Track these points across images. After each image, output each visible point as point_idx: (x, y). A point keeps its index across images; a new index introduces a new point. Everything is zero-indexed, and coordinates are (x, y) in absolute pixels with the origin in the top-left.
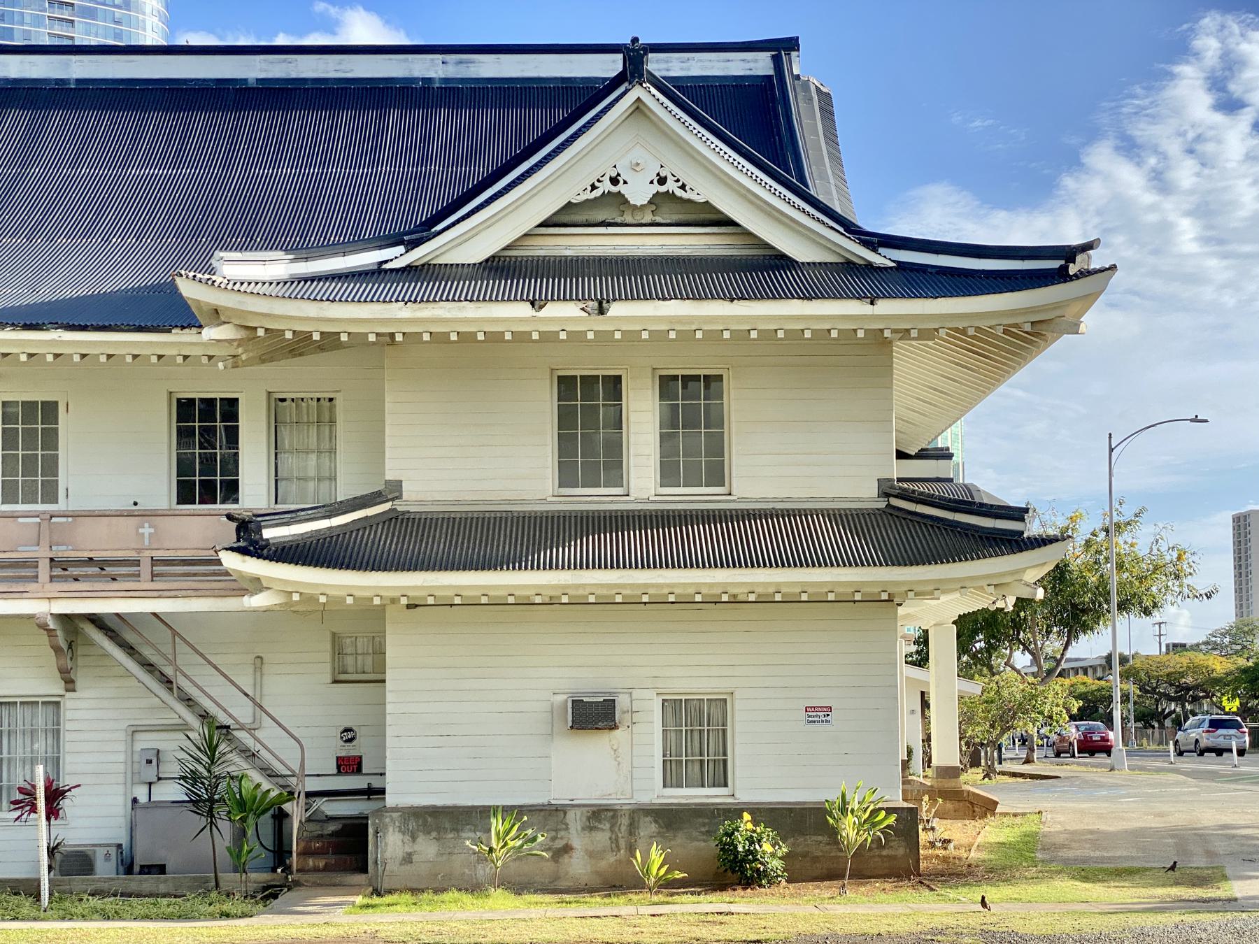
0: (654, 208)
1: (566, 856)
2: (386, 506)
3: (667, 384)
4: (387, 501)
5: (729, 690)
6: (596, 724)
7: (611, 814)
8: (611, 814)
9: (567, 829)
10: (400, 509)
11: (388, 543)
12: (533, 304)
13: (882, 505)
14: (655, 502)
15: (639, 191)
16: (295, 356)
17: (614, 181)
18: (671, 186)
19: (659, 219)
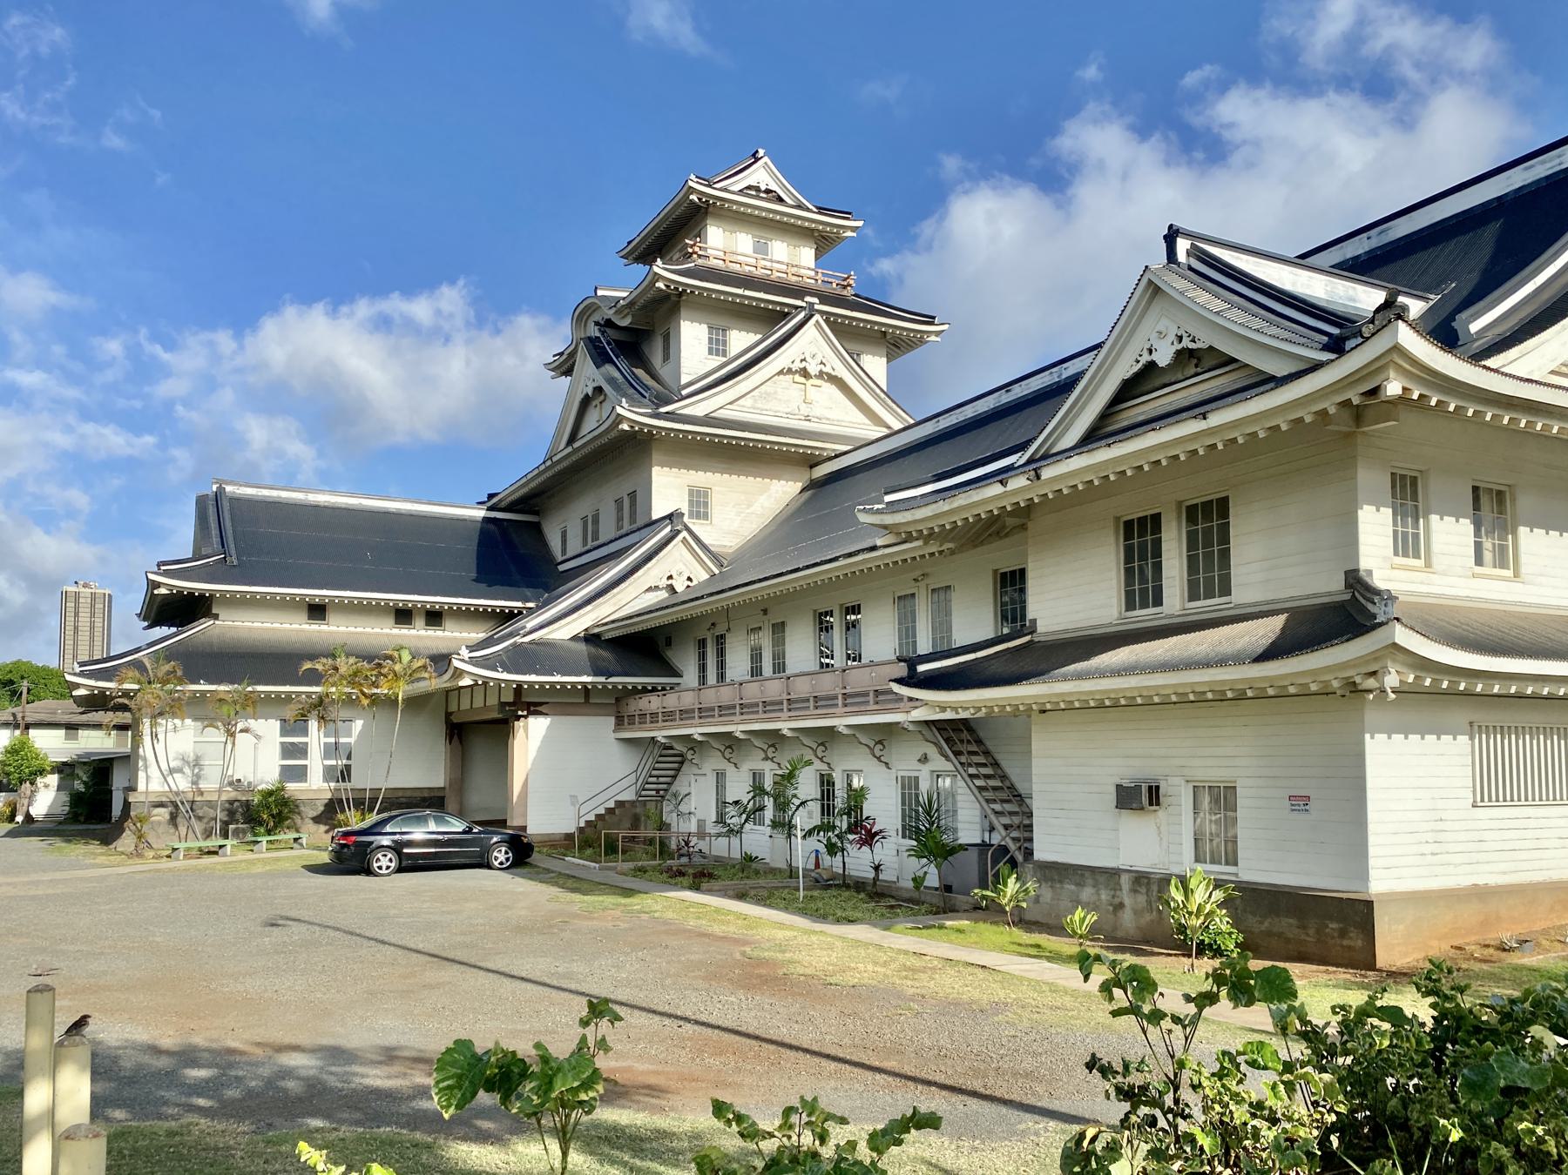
0: (1195, 361)
1: (1121, 912)
2: (1027, 638)
3: (1192, 513)
4: (1026, 635)
5: (1233, 779)
6: (1131, 803)
7: (1146, 881)
8: (1146, 881)
9: (1121, 890)
10: (1036, 640)
11: (997, 668)
12: (1001, 482)
13: (1347, 597)
14: (1179, 616)
15: (1163, 358)
16: (1001, 538)
17: (1150, 352)
18: (1186, 343)
19: (1199, 370)
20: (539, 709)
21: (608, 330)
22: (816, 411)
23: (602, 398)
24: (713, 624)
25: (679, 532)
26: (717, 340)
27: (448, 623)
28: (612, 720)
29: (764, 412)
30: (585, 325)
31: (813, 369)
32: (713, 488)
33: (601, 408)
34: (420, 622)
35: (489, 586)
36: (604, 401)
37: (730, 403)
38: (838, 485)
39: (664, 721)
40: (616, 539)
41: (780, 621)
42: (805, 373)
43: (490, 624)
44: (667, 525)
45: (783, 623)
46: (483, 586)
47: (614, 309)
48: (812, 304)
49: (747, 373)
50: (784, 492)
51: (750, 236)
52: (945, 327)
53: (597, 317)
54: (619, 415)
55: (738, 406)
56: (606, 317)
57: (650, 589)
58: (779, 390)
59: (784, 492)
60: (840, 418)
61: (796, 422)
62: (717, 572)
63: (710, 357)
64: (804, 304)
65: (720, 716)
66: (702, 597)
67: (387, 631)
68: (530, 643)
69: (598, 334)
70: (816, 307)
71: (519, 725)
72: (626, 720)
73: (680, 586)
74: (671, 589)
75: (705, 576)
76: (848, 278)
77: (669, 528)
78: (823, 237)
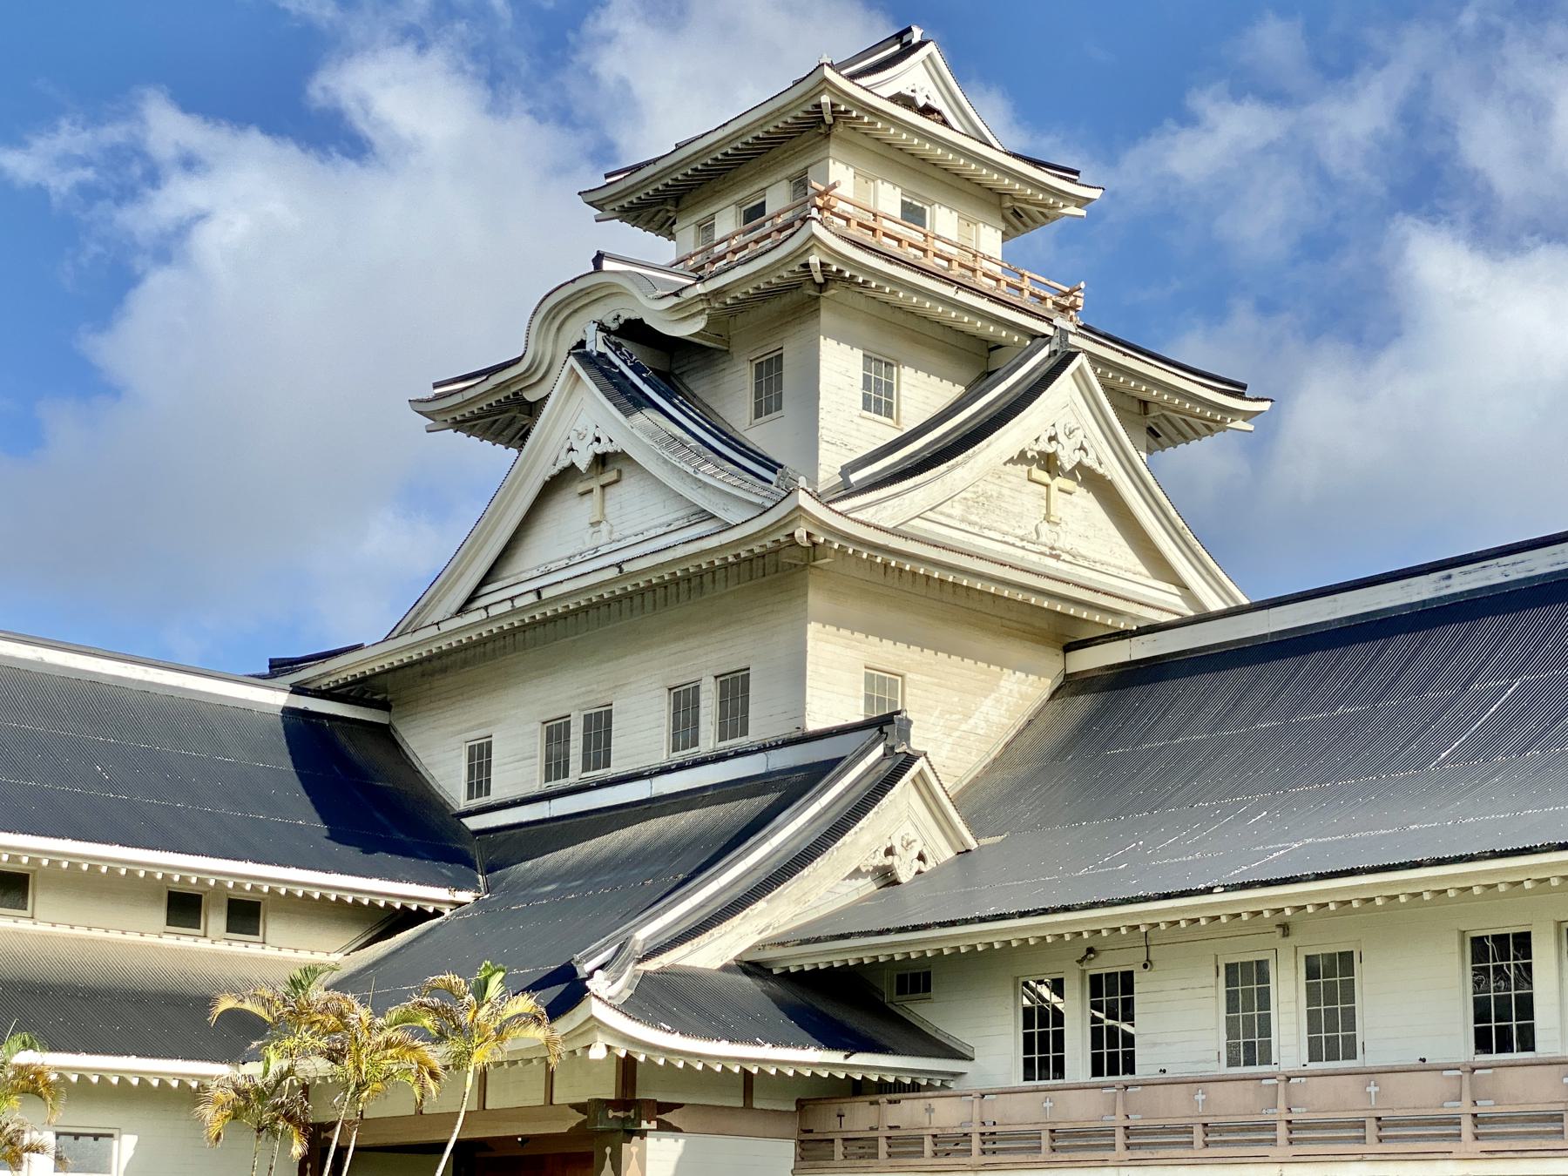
20: (666, 1117)
21: (627, 346)
22: (1065, 542)
23: (610, 476)
24: (1090, 950)
25: (910, 760)
26: (878, 381)
27: (273, 928)
28: (788, 1149)
29: (987, 533)
30: (559, 329)
31: (1068, 459)
32: (909, 676)
33: (603, 495)
34: (216, 921)
35: (368, 850)
36: (616, 482)
37: (931, 510)
38: (1165, 689)
39: (984, 1152)
40: (681, 767)
41: (1350, 950)
42: (1049, 462)
43: (353, 935)
44: (874, 744)
45: (1347, 958)
46: (351, 853)
47: (675, 300)
48: (1064, 333)
49: (970, 452)
50: (1023, 696)
51: (898, 190)
52: (1265, 406)
53: (606, 312)
54: (799, 507)
55: (941, 513)
56: (625, 315)
57: (851, 877)
58: (1006, 492)
59: (1023, 696)
60: (1104, 559)
61: (1035, 557)
62: (972, 844)
63: (866, 413)
64: (1049, 331)
65: (1207, 1145)
66: (1209, 891)
67: (151, 939)
68: (662, 972)
69: (602, 349)
70: (1072, 339)
71: (630, 1149)
72: (839, 1148)
73: (905, 874)
74: (887, 877)
75: (950, 854)
76: (1071, 293)
77: (879, 751)
78: (1015, 213)
